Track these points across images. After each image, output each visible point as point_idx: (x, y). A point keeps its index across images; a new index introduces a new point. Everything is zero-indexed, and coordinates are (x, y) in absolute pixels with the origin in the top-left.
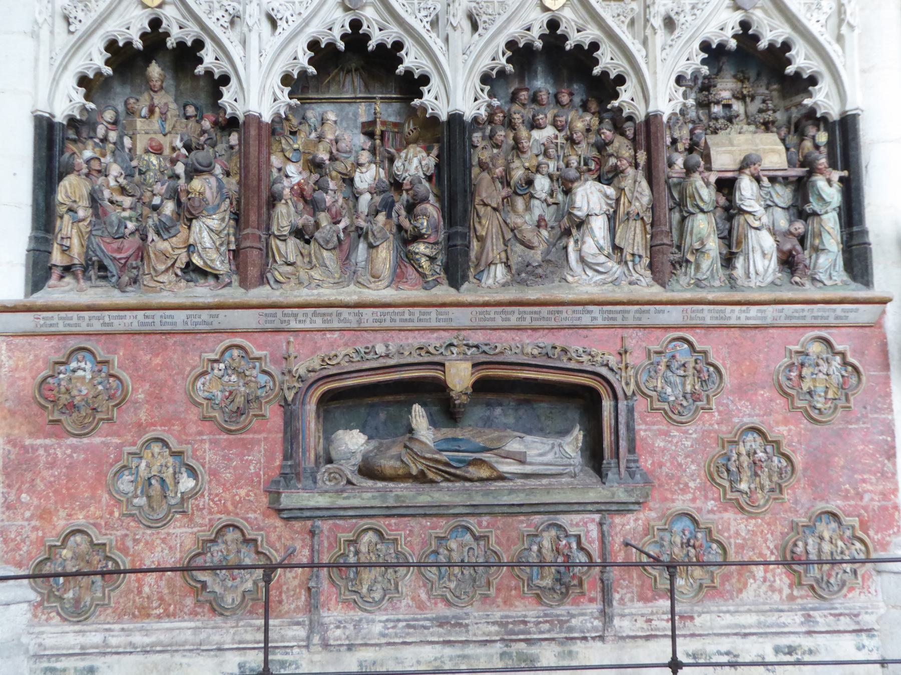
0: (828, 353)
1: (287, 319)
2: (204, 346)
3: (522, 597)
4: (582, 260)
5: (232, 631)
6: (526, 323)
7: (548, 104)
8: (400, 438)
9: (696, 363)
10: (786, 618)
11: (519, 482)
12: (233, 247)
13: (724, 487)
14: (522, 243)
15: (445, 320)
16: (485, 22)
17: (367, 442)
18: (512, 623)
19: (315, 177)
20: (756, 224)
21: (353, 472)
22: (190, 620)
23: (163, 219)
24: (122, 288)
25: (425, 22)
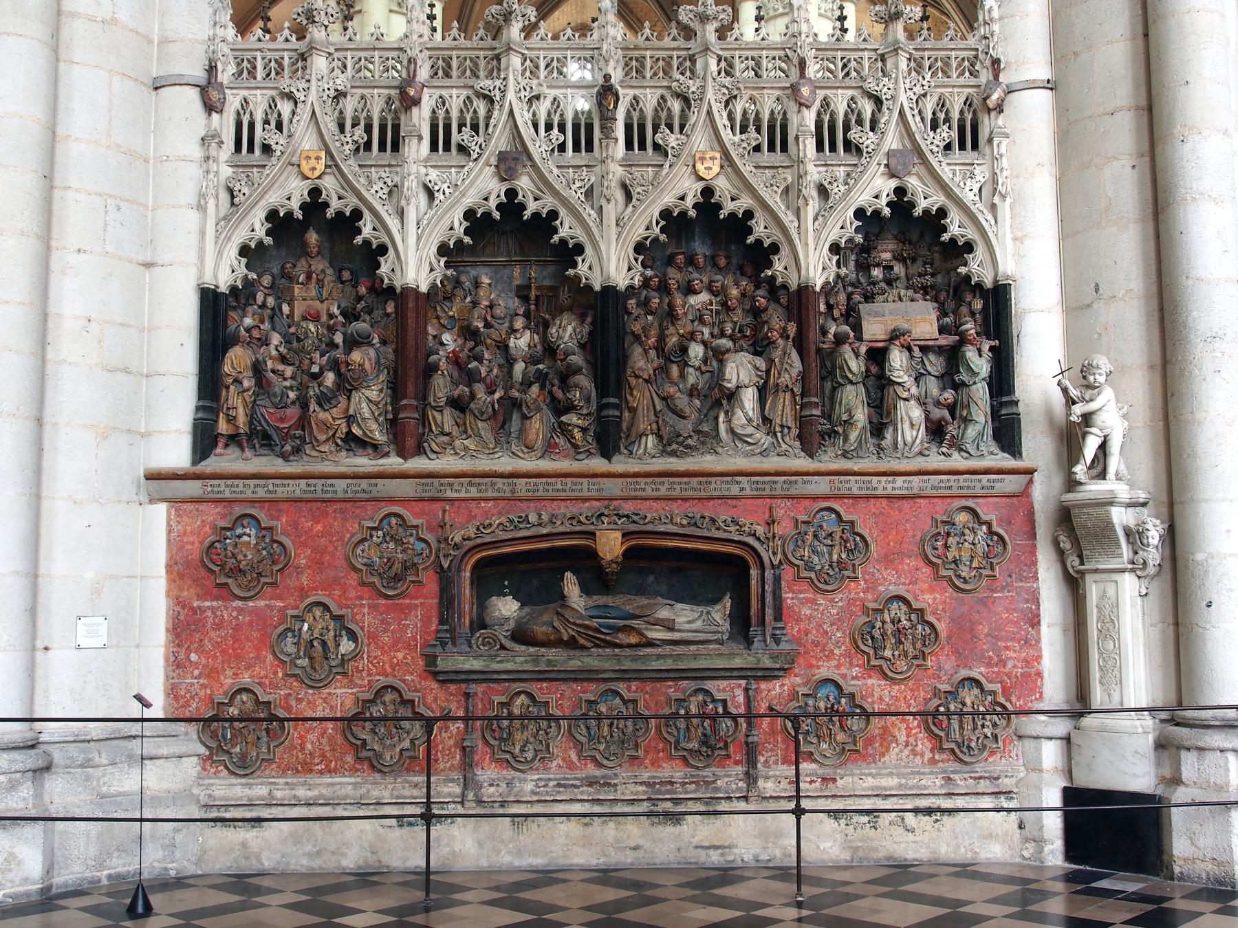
0: (974, 522)
1: (443, 488)
2: (363, 514)
3: (670, 758)
4: (732, 431)
5: (390, 787)
6: (677, 493)
7: (705, 267)
8: (553, 605)
9: (843, 533)
11: (668, 648)
12: (390, 416)
13: (868, 654)
14: (674, 412)
15: (596, 490)
16: (639, 193)
17: (521, 608)
18: (658, 783)
19: (470, 344)
20: (905, 395)
21: (506, 637)
22: (350, 776)
23: (325, 391)
24: (285, 457)
25: (579, 194)
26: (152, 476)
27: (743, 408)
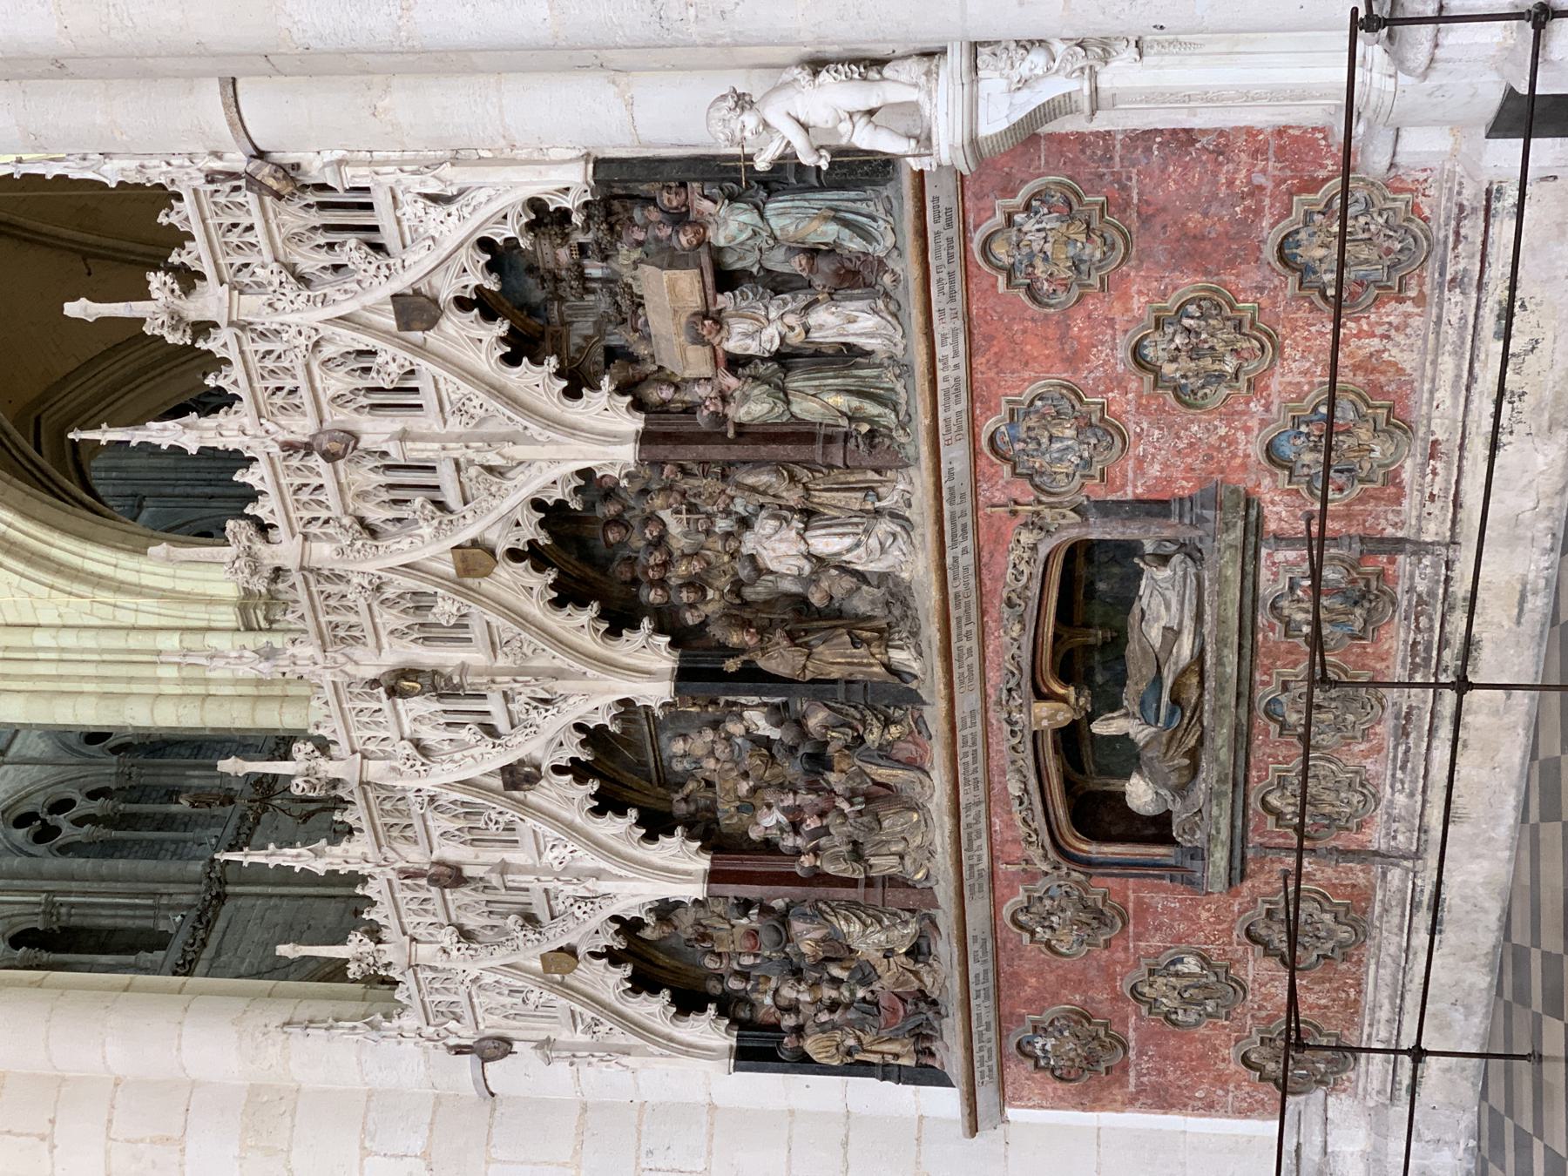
3: (1375, 642)
5: (1385, 934)
6: (974, 628)
10: (1452, 313)
26: (974, 1129)
27: (839, 554)
